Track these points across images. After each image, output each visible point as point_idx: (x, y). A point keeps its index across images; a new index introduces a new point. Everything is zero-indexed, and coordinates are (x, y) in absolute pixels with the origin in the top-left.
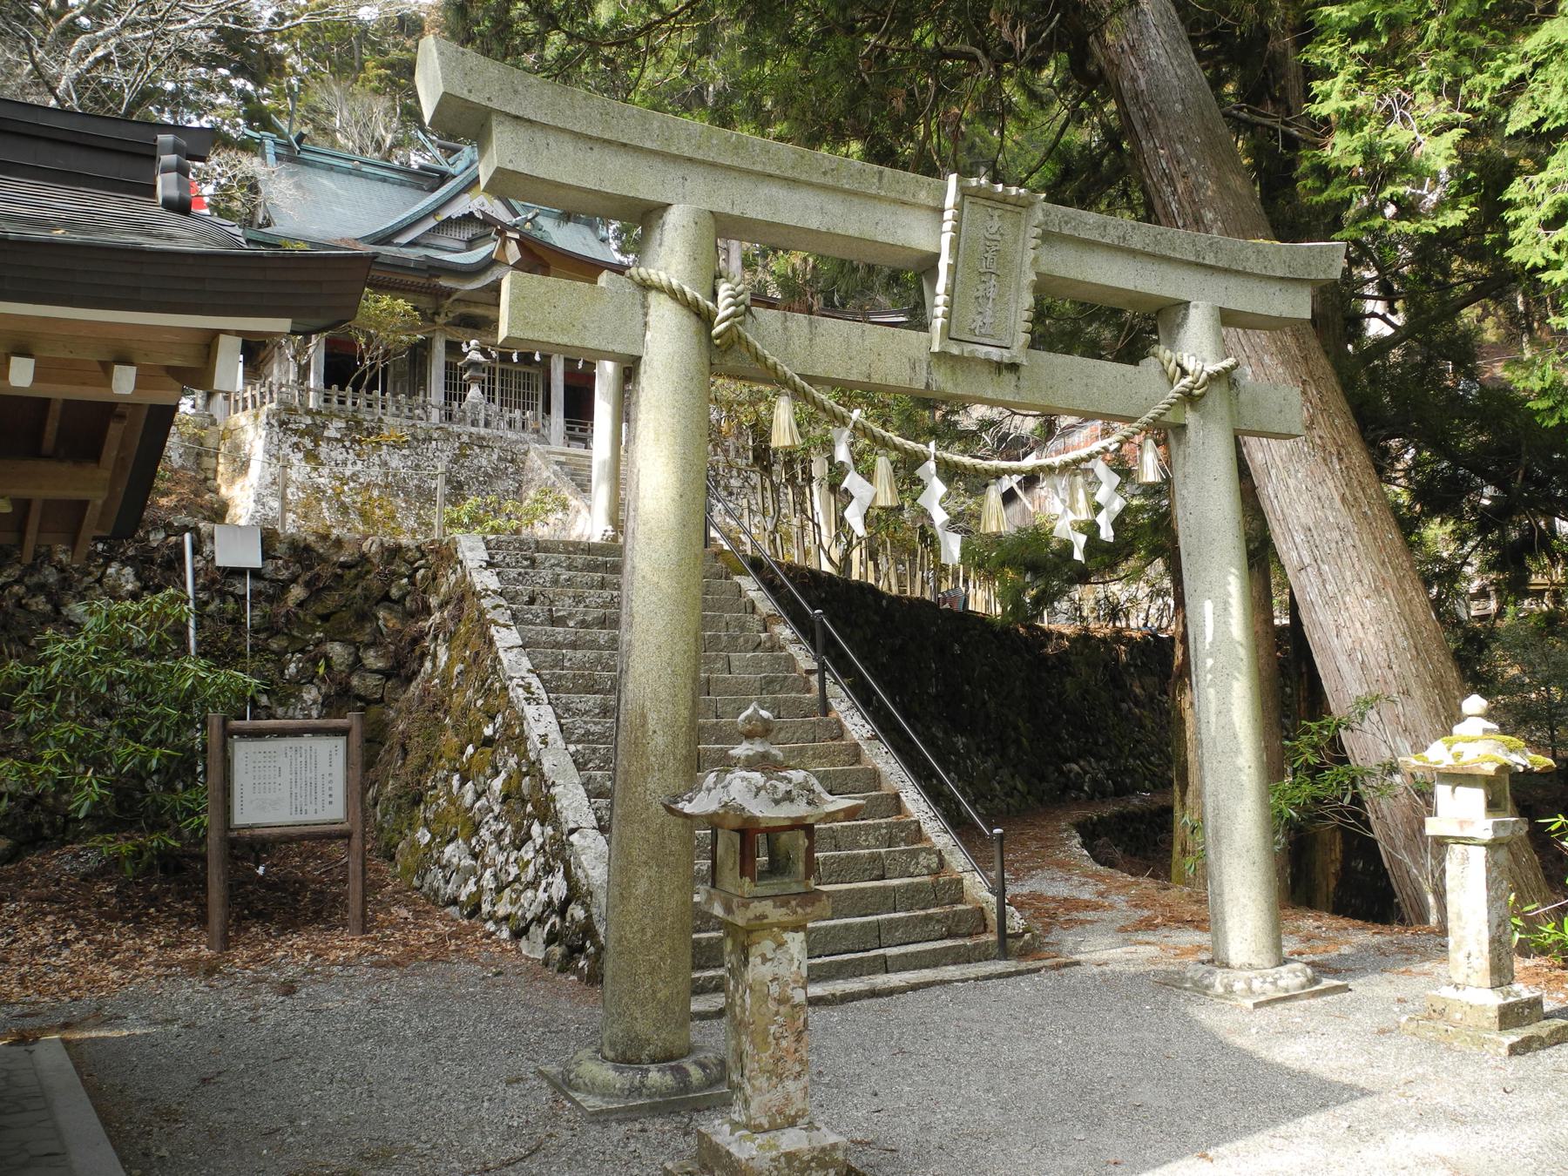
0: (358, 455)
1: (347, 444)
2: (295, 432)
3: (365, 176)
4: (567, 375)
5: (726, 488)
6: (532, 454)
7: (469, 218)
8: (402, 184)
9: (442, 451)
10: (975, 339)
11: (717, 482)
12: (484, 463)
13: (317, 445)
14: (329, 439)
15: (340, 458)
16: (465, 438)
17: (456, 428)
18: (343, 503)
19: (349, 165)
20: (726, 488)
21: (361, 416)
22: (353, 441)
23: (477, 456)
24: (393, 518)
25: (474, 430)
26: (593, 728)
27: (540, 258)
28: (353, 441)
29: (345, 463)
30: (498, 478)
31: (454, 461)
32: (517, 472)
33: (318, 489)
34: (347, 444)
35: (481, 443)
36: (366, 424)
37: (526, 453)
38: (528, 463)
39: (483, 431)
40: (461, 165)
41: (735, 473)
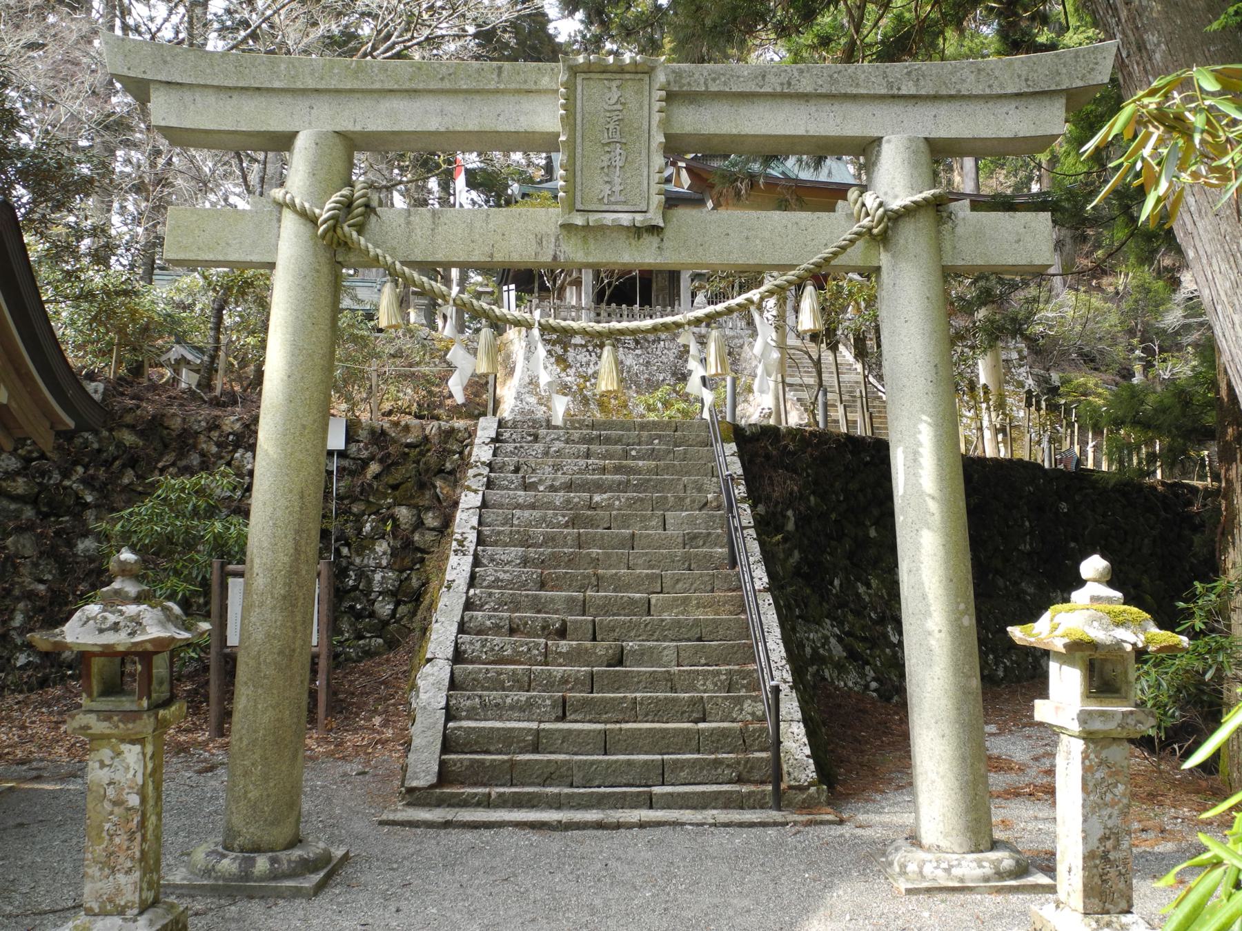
1: (590, 348)
9: (669, 349)
10: (605, 208)
13: (566, 351)
14: (576, 345)
15: (584, 360)
18: (585, 396)
22: (595, 346)
24: (626, 406)
26: (502, 576)
28: (595, 346)
29: (588, 364)
34: (590, 348)
37: (741, 347)
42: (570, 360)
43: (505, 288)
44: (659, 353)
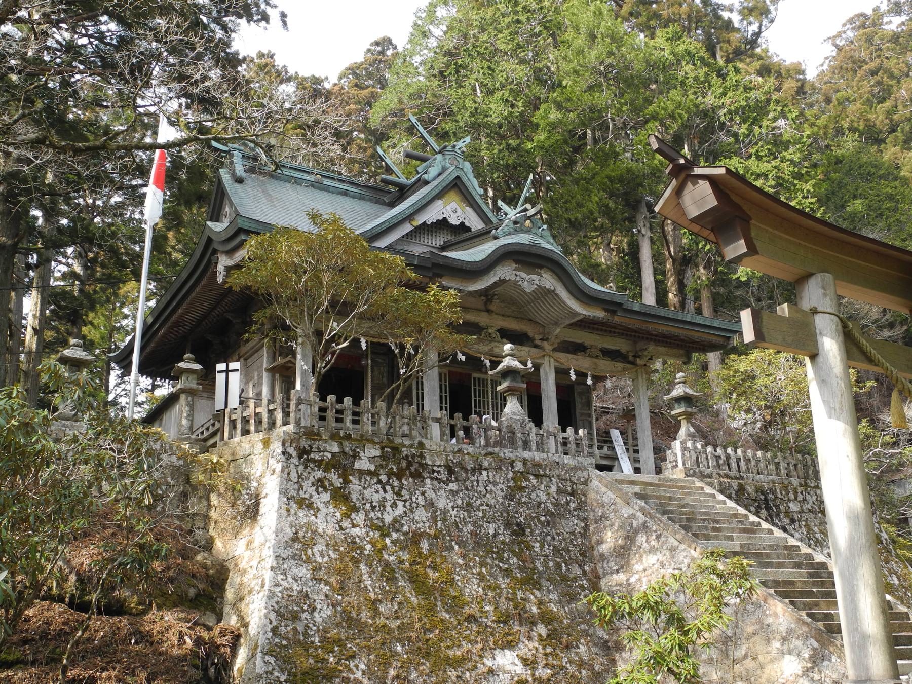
0: (398, 494)
1: (384, 478)
2: (319, 463)
3: (327, 189)
4: (559, 388)
5: (787, 513)
6: (595, 483)
7: (442, 225)
8: (361, 198)
9: (495, 484)
11: (777, 507)
12: (544, 497)
13: (346, 482)
14: (361, 473)
15: (376, 498)
17: (507, 453)
18: (387, 564)
19: (311, 178)
21: (398, 441)
22: (390, 474)
23: (534, 489)
25: (527, 454)
27: (738, 207)
29: (382, 506)
30: (561, 516)
31: (510, 497)
32: (579, 508)
33: (352, 543)
34: (384, 478)
35: (536, 470)
36: (405, 452)
37: (586, 483)
38: (592, 496)
39: (538, 456)
40: (433, 172)
41: (792, 495)
42: (354, 497)
43: (221, 367)
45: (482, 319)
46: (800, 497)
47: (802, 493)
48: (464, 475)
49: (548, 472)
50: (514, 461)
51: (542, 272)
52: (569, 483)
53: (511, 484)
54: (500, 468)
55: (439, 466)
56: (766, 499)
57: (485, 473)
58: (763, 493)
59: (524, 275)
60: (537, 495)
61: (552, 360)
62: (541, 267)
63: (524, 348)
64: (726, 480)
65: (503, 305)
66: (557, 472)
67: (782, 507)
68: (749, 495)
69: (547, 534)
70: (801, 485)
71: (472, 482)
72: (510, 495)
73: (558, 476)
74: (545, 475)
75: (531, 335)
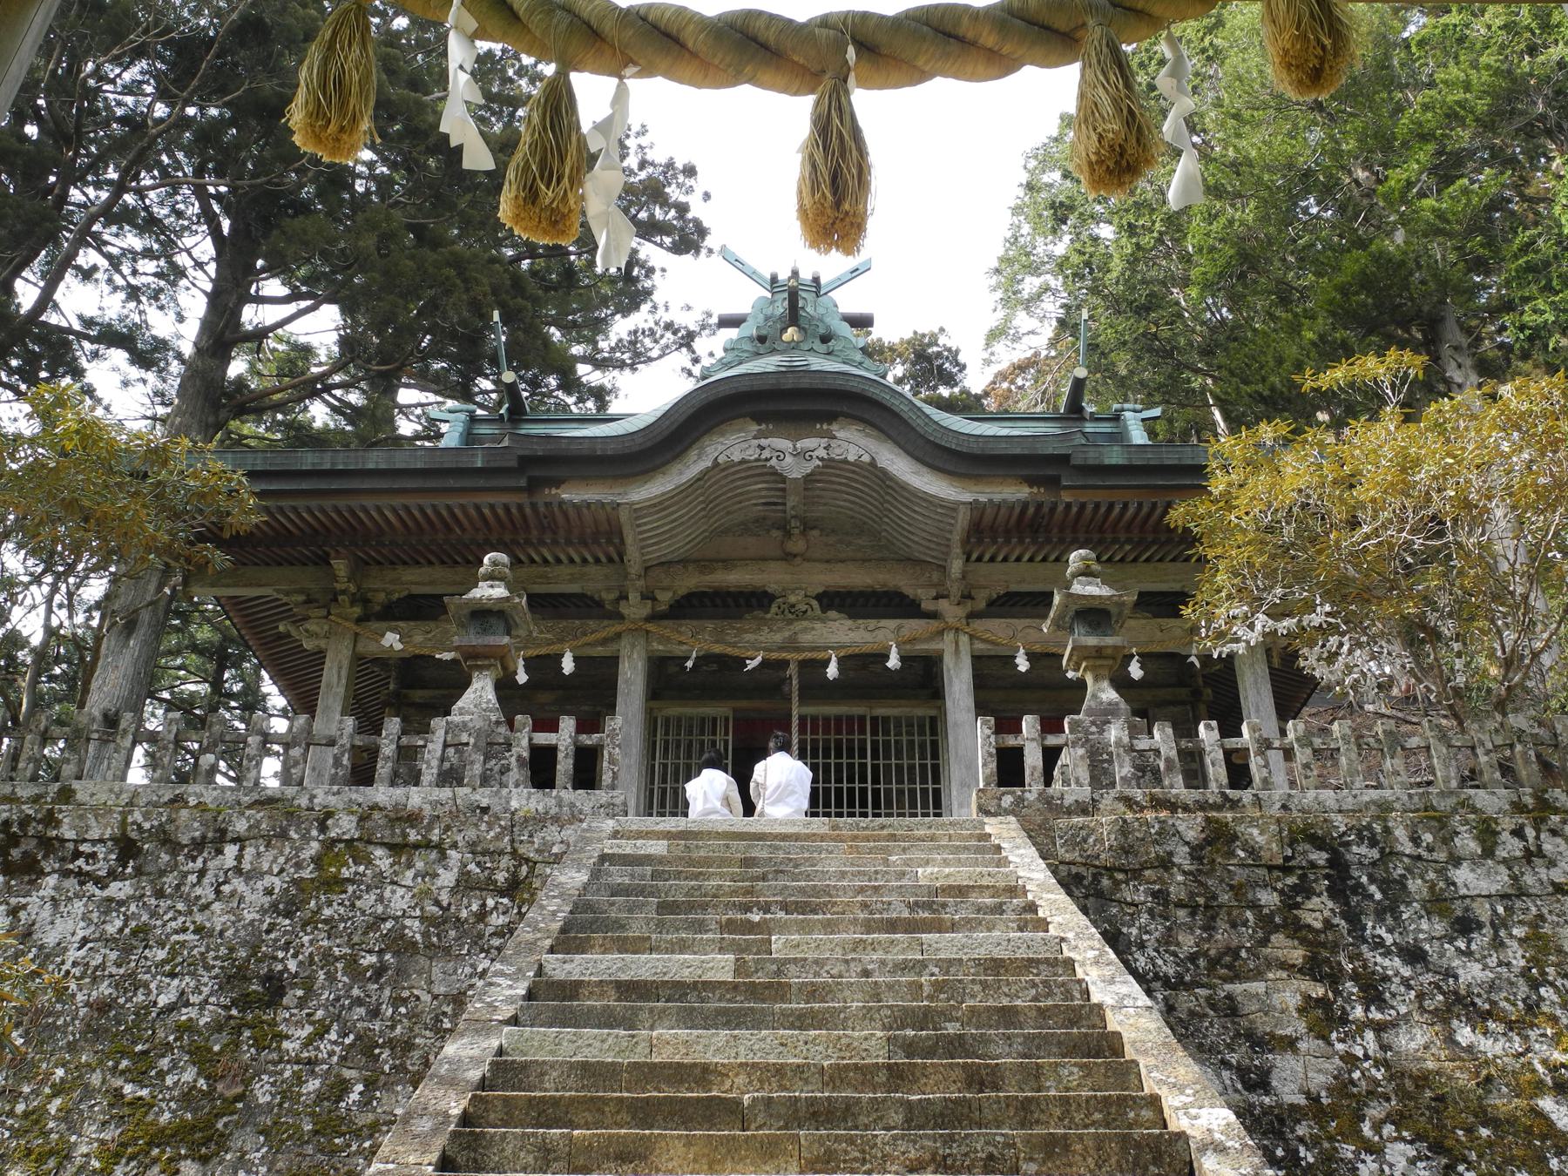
12: (399, 900)
16: (345, 826)
20: (1437, 903)
31: (287, 905)
41: (1467, 843)
44: (206, 892)
45: (770, 577)
46: (1510, 846)
47: (1518, 833)
48: (165, 857)
49: (435, 836)
50: (329, 815)
51: (834, 427)
52: (505, 861)
53: (307, 873)
54: (283, 835)
55: (94, 842)
56: (1338, 865)
57: (231, 851)
58: (1319, 842)
59: (784, 444)
60: (380, 899)
61: (964, 639)
62: (831, 417)
63: (884, 623)
64: (1150, 815)
65: (832, 539)
66: (471, 834)
67: (1415, 885)
68: (1252, 852)
69: (359, 1002)
70: (1518, 807)
71: (185, 875)
72: (291, 902)
73: (473, 847)
74: (427, 845)
75: (909, 591)
